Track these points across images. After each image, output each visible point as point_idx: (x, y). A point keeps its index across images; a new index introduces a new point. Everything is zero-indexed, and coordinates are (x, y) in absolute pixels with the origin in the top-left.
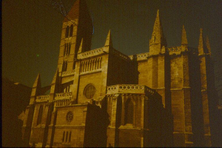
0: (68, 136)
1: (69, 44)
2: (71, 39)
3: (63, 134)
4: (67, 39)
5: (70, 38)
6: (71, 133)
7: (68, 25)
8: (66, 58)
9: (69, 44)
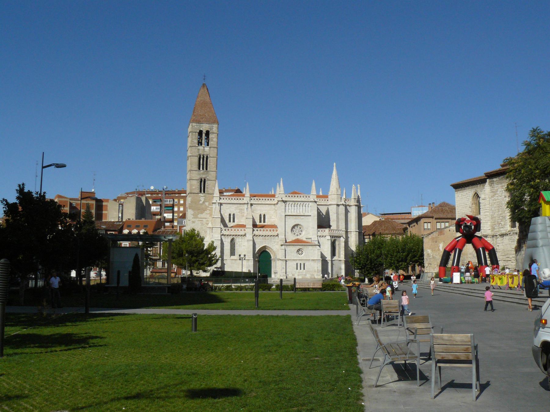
0: (302, 266)
1: (205, 156)
2: (210, 150)
4: (203, 148)
5: (207, 149)
6: (304, 264)
7: (201, 129)
8: (203, 174)
9: (205, 156)
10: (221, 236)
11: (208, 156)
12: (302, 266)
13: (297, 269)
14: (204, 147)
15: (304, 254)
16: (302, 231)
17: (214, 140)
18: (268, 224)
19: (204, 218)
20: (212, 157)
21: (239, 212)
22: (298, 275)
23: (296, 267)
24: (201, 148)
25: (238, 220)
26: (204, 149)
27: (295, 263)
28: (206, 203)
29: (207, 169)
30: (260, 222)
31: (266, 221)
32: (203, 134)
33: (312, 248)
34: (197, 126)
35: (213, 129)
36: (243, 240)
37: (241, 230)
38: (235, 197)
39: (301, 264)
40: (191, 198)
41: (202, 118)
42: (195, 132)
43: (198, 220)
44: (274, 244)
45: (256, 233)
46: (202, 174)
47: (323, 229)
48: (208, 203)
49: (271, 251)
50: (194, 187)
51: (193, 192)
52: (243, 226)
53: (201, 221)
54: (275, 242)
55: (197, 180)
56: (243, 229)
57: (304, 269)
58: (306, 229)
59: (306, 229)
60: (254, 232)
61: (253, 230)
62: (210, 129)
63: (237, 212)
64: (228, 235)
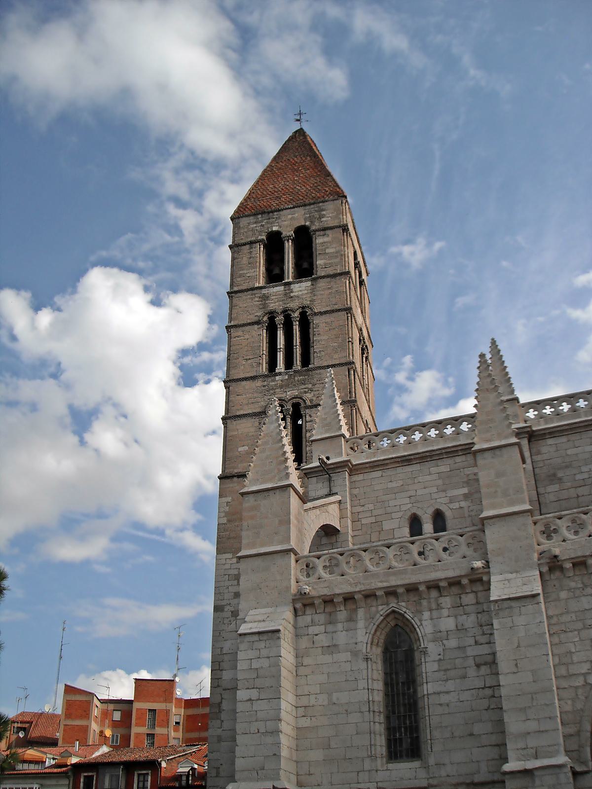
2: (313, 291)
4: (282, 288)
5: (301, 288)
7: (275, 229)
14: (289, 284)
17: (327, 251)
20: (326, 312)
21: (466, 497)
24: (278, 289)
26: (288, 295)
29: (306, 361)
34: (256, 223)
40: (229, 499)
46: (281, 387)
64: (349, 598)
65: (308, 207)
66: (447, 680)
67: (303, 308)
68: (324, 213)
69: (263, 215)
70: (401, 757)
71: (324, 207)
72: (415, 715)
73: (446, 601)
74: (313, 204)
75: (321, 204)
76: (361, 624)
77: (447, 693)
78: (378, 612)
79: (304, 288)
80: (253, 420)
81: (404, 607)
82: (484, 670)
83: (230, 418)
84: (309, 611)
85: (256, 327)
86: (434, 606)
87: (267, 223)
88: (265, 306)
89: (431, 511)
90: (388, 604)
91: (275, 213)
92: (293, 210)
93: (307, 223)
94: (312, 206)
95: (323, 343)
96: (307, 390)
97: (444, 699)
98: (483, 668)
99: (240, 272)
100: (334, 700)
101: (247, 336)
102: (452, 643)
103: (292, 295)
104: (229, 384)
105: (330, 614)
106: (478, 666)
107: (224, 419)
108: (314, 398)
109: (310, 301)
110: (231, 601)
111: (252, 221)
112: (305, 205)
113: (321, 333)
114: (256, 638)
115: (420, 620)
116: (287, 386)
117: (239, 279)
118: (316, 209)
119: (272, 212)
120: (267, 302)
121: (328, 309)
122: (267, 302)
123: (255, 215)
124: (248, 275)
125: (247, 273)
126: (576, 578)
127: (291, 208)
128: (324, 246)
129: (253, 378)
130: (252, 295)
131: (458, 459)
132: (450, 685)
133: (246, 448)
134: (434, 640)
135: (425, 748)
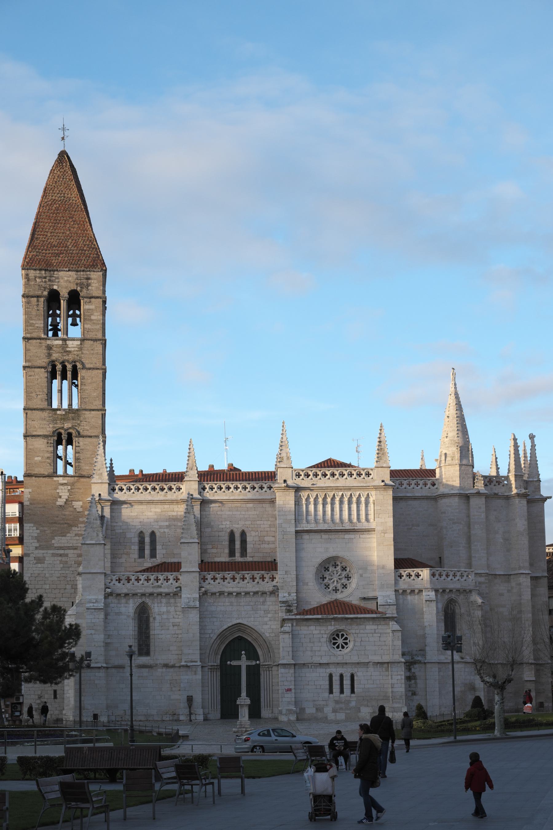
0: (347, 682)
1: (69, 367)
2: (81, 349)
3: (327, 678)
4: (60, 342)
6: (352, 677)
7: (55, 287)
9: (69, 367)
10: (105, 598)
11: (79, 366)
12: (347, 682)
13: (331, 692)
15: (351, 645)
16: (348, 578)
17: (93, 317)
18: (256, 559)
19: (69, 548)
20: (90, 369)
22: (335, 711)
23: (328, 687)
25: (164, 551)
27: (324, 673)
28: (74, 503)
30: (232, 553)
31: (249, 551)
32: (62, 301)
33: (375, 627)
35: (88, 285)
36: (172, 609)
37: (167, 580)
38: (154, 484)
39: (341, 676)
41: (58, 255)
42: (38, 297)
43: (54, 555)
44: (266, 619)
45: (213, 586)
47: (413, 571)
48: (81, 503)
49: (255, 640)
50: (38, 459)
51: (37, 471)
52: (175, 567)
53: (61, 555)
54: (267, 612)
55: (45, 436)
56: (171, 576)
57: (353, 691)
58: (360, 572)
59: (360, 572)
60: (204, 584)
61: (204, 579)
62: (81, 285)
63: (161, 527)
64: (126, 595)
65: (79, 273)
66: (162, 630)
67: (75, 362)
68: (90, 281)
69: (46, 272)
70: (143, 655)
71: (90, 276)
72: (149, 640)
73: (164, 600)
74: (83, 271)
75: (88, 273)
76: (131, 605)
77: (162, 634)
78: (138, 601)
79: (75, 346)
80: (43, 440)
81: (148, 600)
82: (176, 628)
83: (28, 436)
84: (110, 597)
85: (43, 370)
86: (159, 601)
87: (50, 280)
88: (49, 355)
89: (150, 531)
90: (142, 599)
91: (56, 273)
92: (68, 273)
93: (79, 289)
94: (82, 273)
95: (87, 392)
96: (77, 424)
97: (160, 636)
98: (175, 627)
99: (31, 322)
100: (120, 633)
101: (37, 377)
102: (165, 616)
103: (68, 349)
104: (27, 411)
105: (119, 600)
106: (173, 626)
107: (26, 436)
108: (81, 431)
109: (80, 357)
110: (34, 552)
111: (38, 275)
112: (77, 271)
113: (86, 384)
114: (93, 610)
115: (154, 607)
116: (64, 419)
117: (31, 328)
118: (86, 276)
119: (54, 271)
120: (51, 352)
121: (92, 366)
122: (51, 352)
123: (40, 270)
124: (37, 325)
125: (35, 324)
126: (212, 599)
127: (66, 271)
128: (89, 312)
129: (42, 410)
130: (40, 343)
131: (166, 506)
132: (163, 632)
133: (40, 458)
134: (159, 614)
135: (152, 653)
